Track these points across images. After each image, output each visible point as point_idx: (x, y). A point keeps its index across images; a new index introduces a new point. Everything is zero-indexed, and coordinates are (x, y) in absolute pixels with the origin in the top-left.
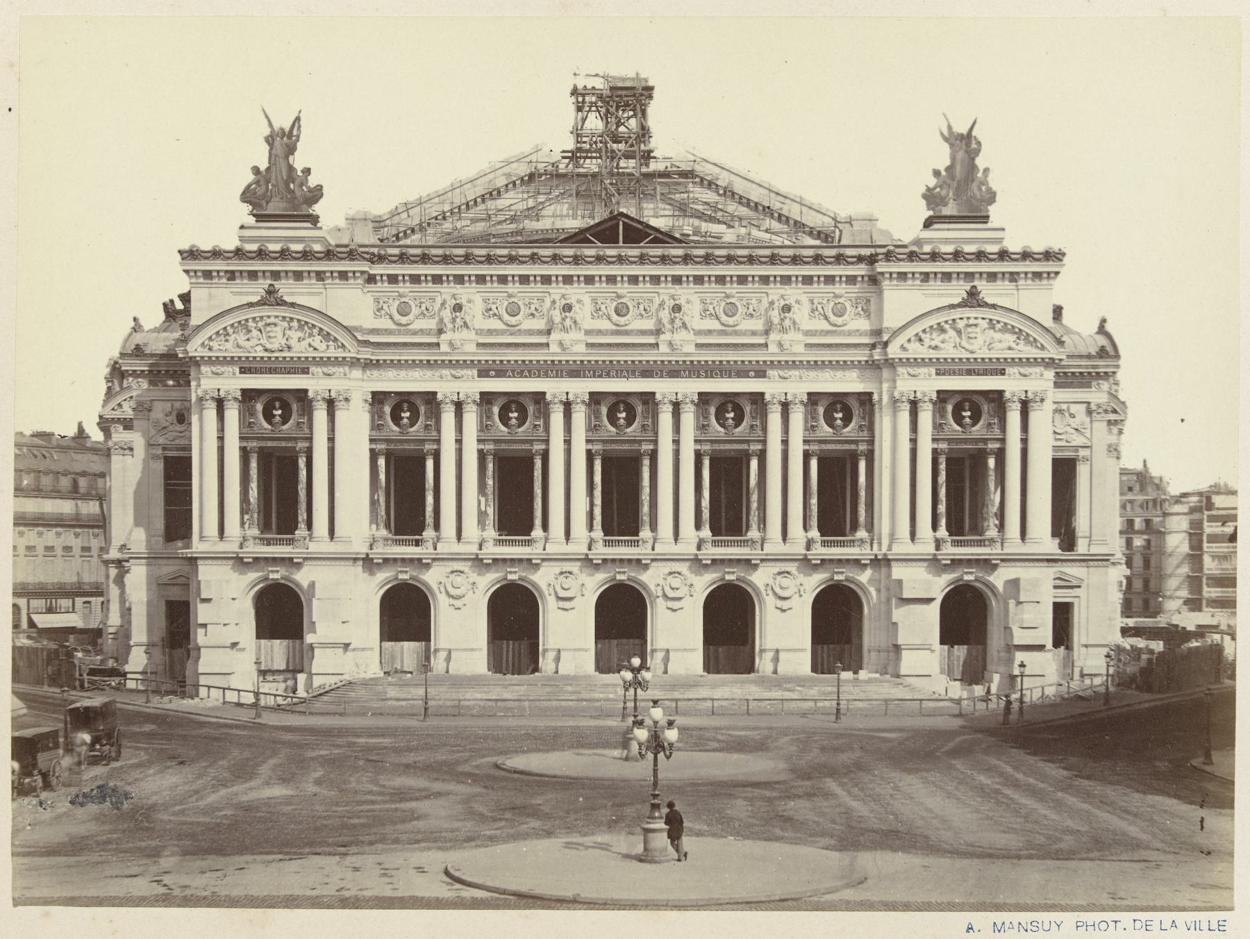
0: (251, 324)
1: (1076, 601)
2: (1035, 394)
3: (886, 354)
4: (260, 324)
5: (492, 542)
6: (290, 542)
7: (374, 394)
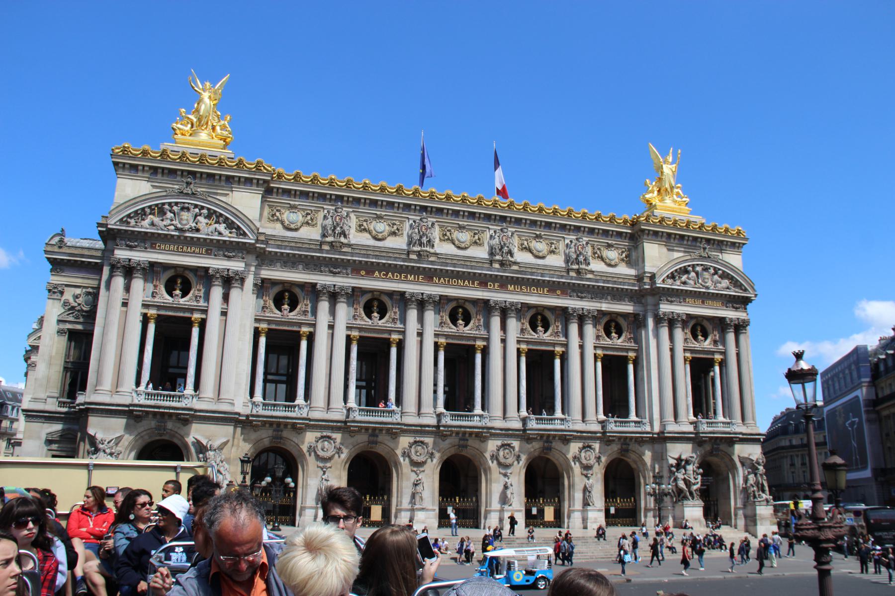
4: (175, 208)
7: (263, 280)
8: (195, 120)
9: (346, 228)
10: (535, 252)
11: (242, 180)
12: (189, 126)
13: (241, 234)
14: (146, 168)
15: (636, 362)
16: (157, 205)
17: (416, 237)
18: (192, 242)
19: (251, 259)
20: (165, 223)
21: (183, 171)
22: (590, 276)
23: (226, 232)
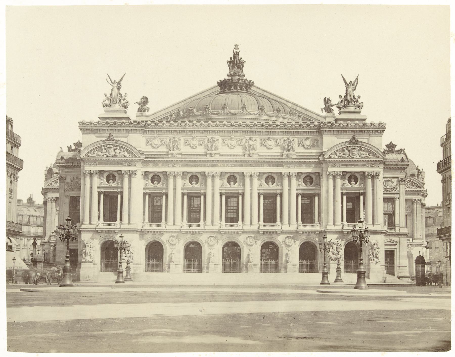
0: (103, 147)
1: (395, 250)
2: (376, 173)
3: (324, 158)
4: (106, 147)
5: (186, 225)
6: (114, 225)
7: (145, 172)
9: (178, 146)
10: (268, 146)
12: (109, 101)
15: (319, 195)
16: (99, 147)
17: (210, 146)
19: (139, 164)
20: (104, 154)
22: (295, 157)
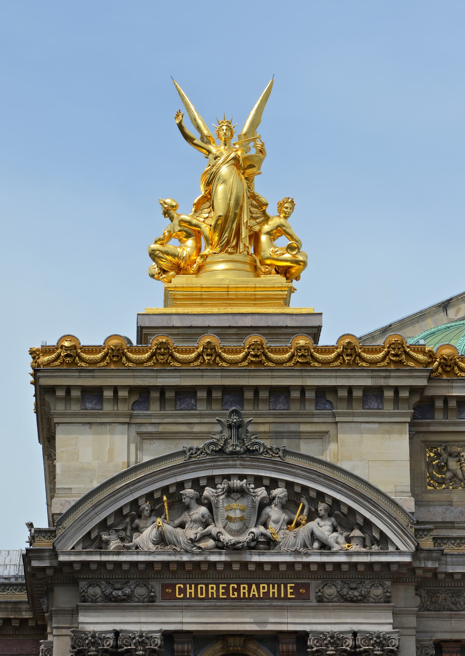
4: (208, 492)
8: (206, 229)
11: (358, 394)
13: (374, 541)
14: (123, 394)
16: (165, 490)
18: (261, 572)
19: (406, 597)
21: (209, 389)
23: (336, 539)
